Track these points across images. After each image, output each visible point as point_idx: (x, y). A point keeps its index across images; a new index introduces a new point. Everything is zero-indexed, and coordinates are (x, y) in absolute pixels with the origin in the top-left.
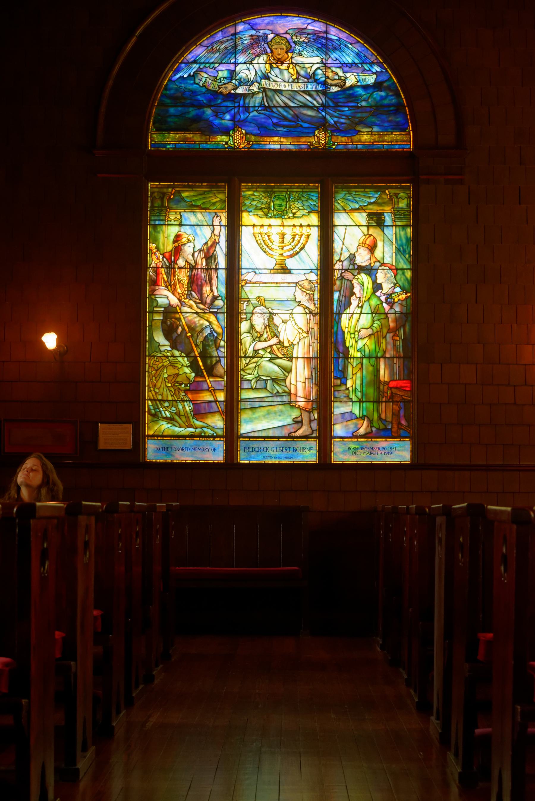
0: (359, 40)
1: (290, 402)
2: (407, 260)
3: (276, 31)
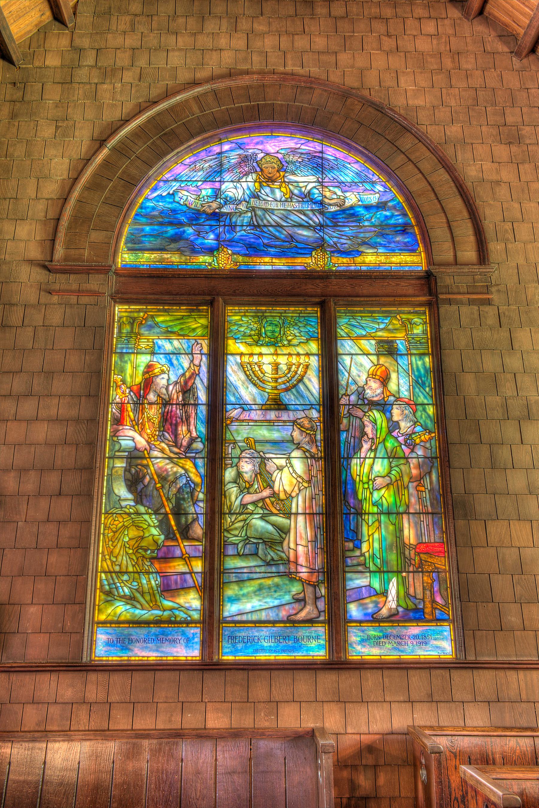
2: (428, 394)
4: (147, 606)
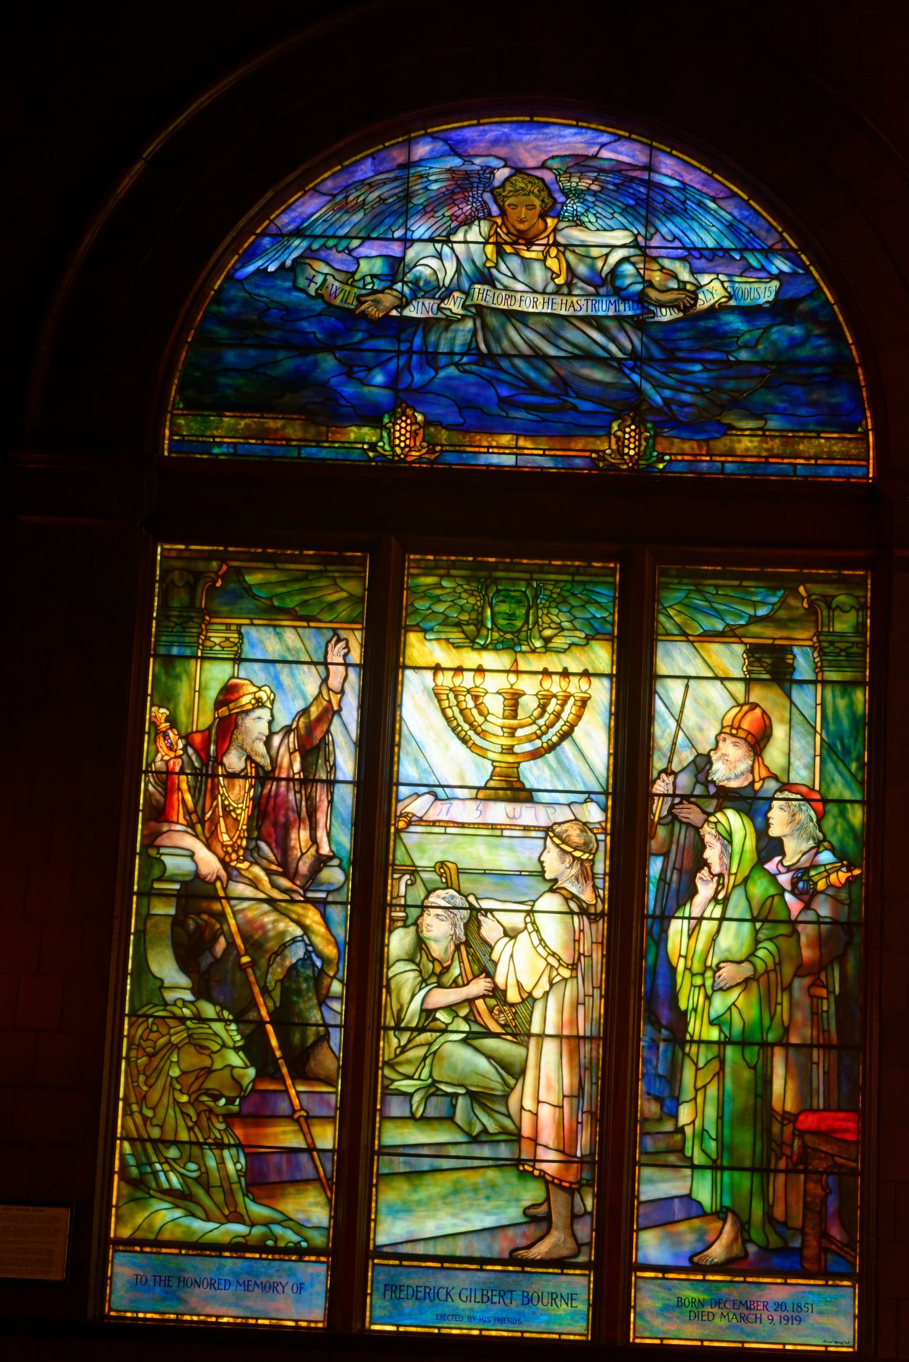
0: (735, 189)
1: (517, 1162)
2: (854, 776)
3: (515, 159)
4: (217, 1213)
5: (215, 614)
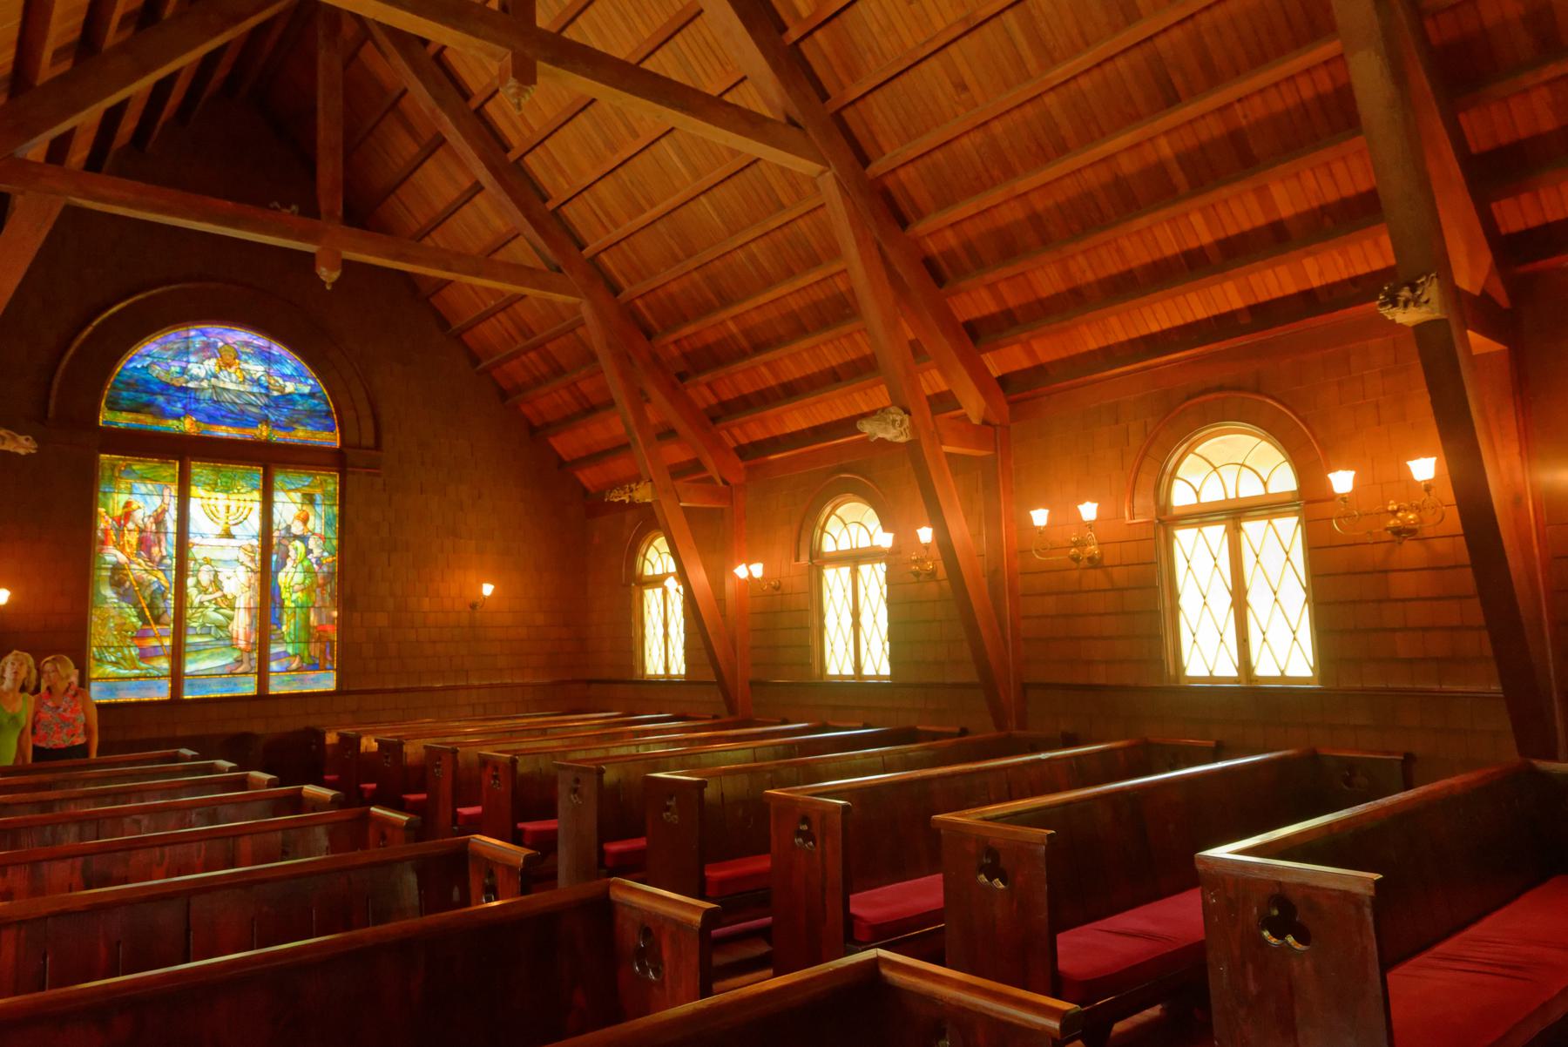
5: (121, 478)
